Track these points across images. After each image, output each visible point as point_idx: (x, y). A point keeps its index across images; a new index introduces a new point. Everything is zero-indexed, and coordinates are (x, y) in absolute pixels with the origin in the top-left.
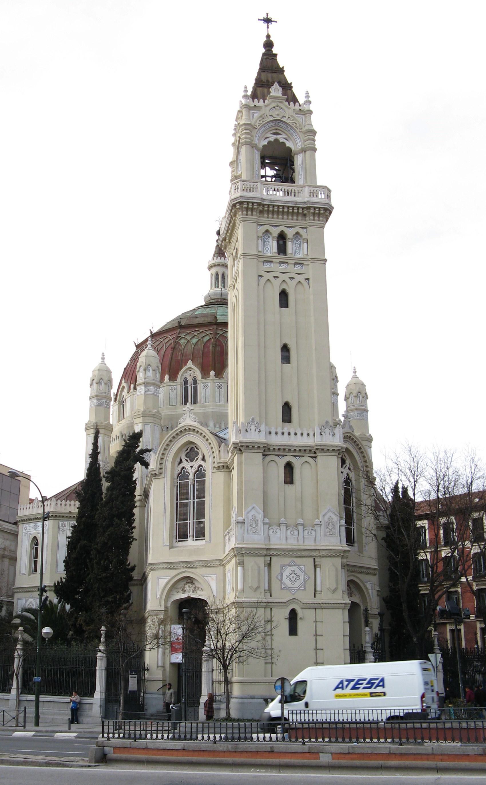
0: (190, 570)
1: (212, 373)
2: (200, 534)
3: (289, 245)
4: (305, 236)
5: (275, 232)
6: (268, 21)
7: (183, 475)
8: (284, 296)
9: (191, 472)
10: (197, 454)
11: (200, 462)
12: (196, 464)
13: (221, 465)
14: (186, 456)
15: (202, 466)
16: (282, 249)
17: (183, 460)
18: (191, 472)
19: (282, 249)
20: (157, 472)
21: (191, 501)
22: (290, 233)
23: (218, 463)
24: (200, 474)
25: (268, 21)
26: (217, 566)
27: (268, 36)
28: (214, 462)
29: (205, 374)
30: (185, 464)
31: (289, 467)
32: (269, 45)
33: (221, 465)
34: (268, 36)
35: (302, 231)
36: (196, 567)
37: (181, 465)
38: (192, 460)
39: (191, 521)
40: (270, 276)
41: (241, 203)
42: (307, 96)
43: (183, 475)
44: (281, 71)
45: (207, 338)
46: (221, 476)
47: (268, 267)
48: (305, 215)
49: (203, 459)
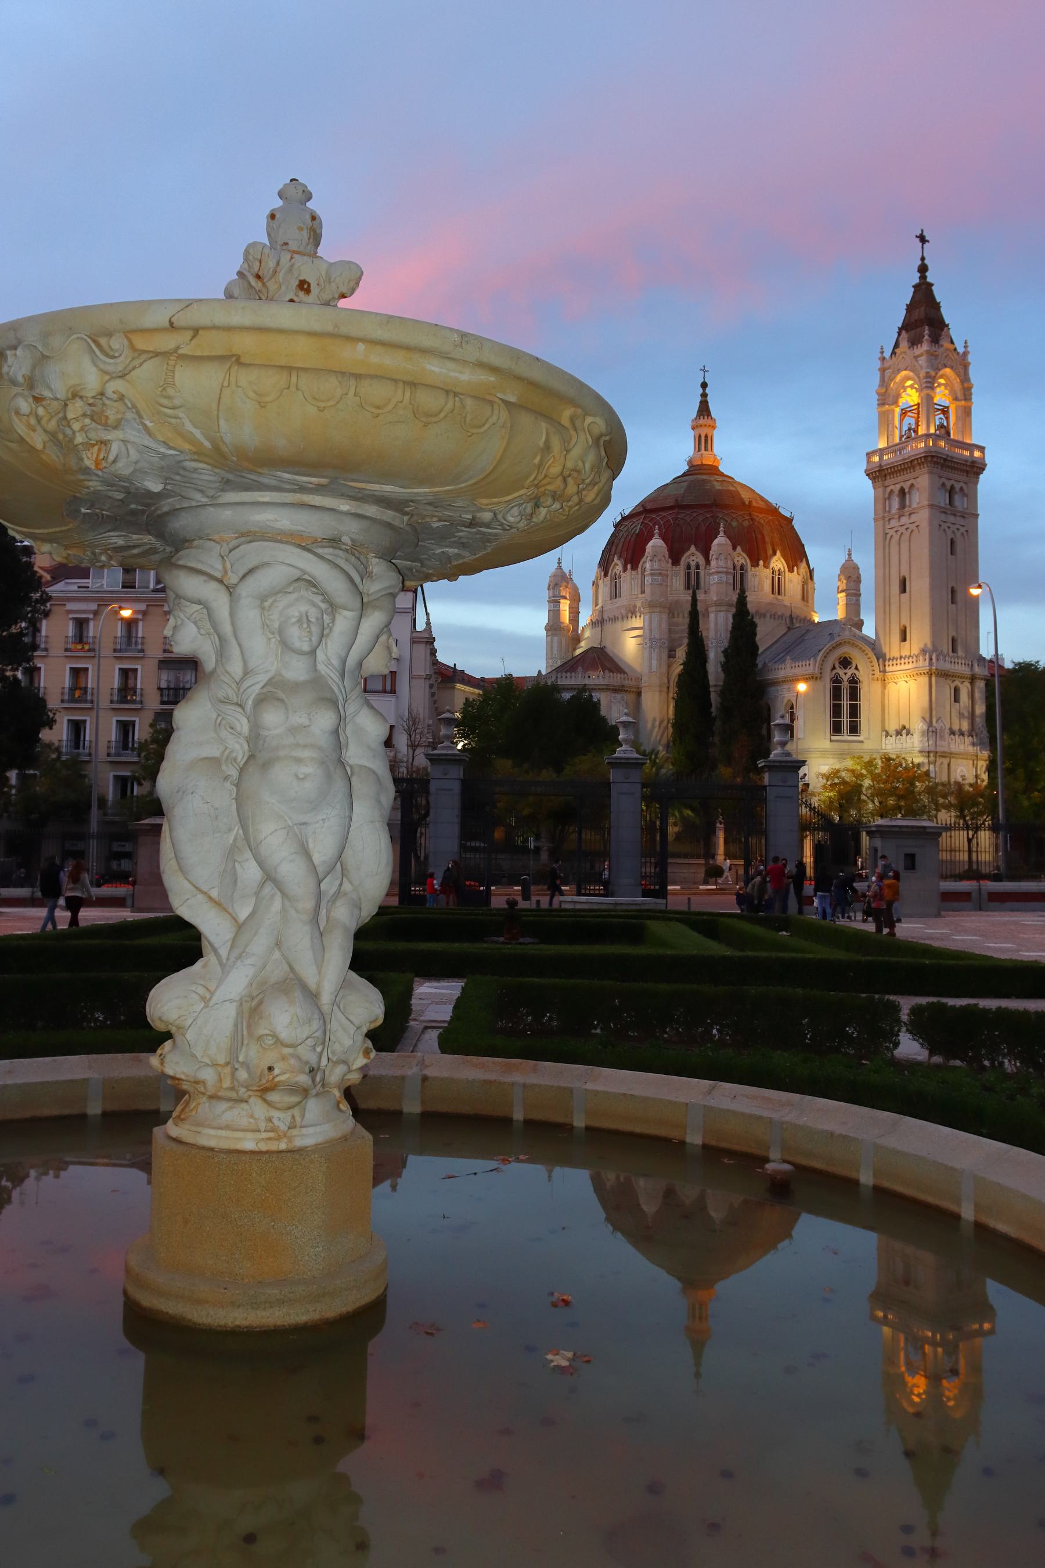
1: (761, 563)
2: (854, 729)
3: (957, 499)
4: (966, 491)
5: (948, 484)
6: (922, 239)
7: (836, 680)
8: (952, 542)
9: (845, 678)
10: (850, 663)
11: (852, 671)
14: (840, 663)
16: (951, 503)
17: (837, 665)
18: (845, 678)
19: (951, 503)
21: (845, 703)
22: (957, 486)
24: (854, 681)
25: (922, 239)
27: (923, 259)
29: (755, 564)
31: (956, 690)
32: (923, 269)
34: (923, 259)
35: (965, 487)
37: (835, 672)
38: (845, 668)
40: (944, 526)
41: (933, 457)
42: (965, 347)
43: (836, 680)
44: (937, 306)
45: (746, 524)
47: (943, 517)
48: (967, 472)
49: (856, 668)
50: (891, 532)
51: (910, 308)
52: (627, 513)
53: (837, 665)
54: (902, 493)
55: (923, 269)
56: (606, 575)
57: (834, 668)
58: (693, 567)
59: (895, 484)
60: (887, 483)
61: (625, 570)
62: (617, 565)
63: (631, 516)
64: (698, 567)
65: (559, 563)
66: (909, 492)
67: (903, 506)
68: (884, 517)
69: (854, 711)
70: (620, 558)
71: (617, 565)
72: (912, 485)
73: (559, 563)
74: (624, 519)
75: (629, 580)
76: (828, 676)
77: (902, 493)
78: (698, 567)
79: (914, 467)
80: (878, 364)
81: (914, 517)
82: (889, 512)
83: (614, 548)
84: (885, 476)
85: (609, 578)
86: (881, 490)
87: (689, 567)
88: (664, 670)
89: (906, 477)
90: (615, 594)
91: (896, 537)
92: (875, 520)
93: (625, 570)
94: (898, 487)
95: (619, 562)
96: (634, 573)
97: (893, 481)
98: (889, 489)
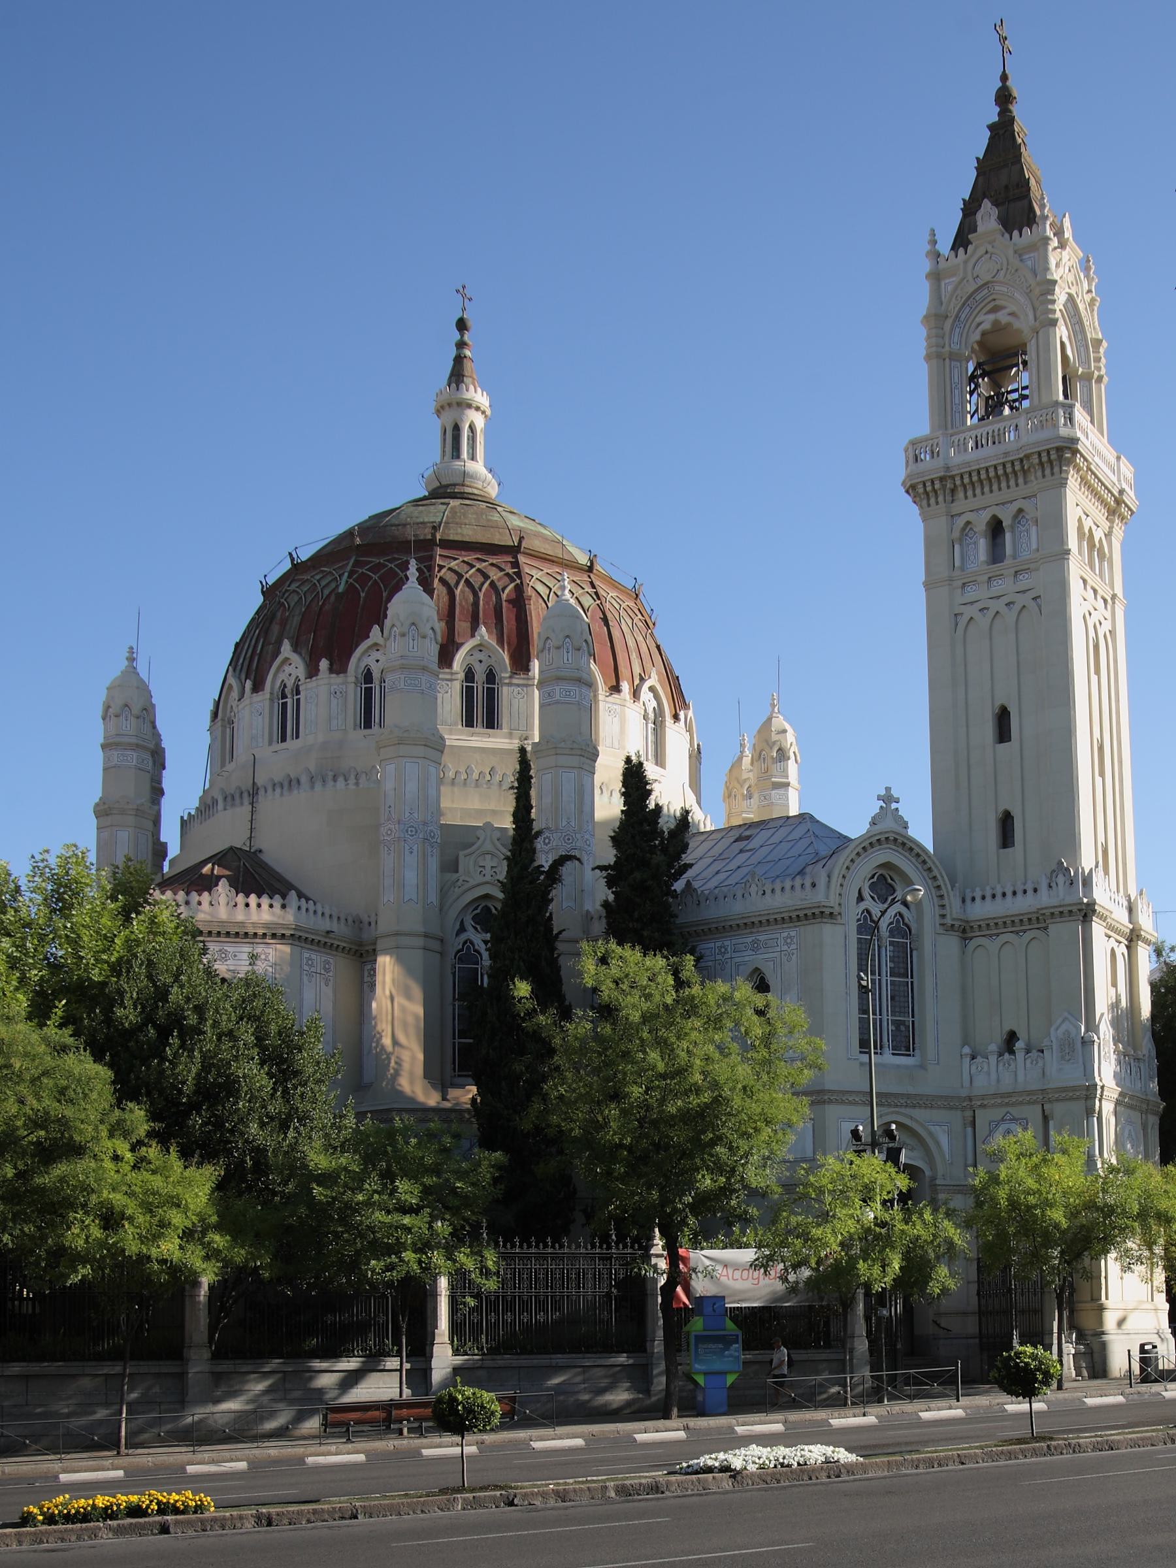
0: (908, 1111)
12: (892, 912)
13: (957, 924)
14: (872, 887)
15: (901, 915)
17: (866, 893)
20: (836, 910)
23: (954, 919)
24: (901, 929)
26: (951, 1108)
27: (1004, 77)
28: (943, 916)
30: (868, 903)
33: (957, 924)
34: (1004, 77)
36: (914, 1107)
37: (863, 905)
39: (885, 1018)
43: (868, 926)
46: (951, 943)
50: (969, 611)
51: (984, 167)
52: (304, 555)
53: (866, 893)
54: (996, 529)
55: (1004, 98)
56: (257, 687)
57: (860, 898)
58: (480, 677)
59: (978, 510)
60: (957, 507)
61: (312, 672)
62: (289, 665)
63: (318, 560)
64: (491, 677)
65: (132, 659)
66: (1012, 527)
67: (996, 554)
68: (951, 580)
69: (904, 998)
70: (296, 648)
71: (289, 665)
72: (1020, 511)
73: (132, 659)
74: (298, 568)
75: (326, 697)
76: (852, 913)
77: (996, 529)
78: (491, 677)
79: (1025, 472)
80: (926, 266)
81: (1025, 581)
82: (962, 569)
83: (275, 629)
84: (953, 491)
85: (265, 695)
86: (943, 521)
87: (469, 675)
88: (433, 898)
89: (1005, 495)
90: (286, 725)
91: (983, 621)
92: (928, 585)
93: (312, 672)
94: (985, 516)
95: (296, 659)
96: (337, 679)
97: (973, 503)
98: (960, 522)
